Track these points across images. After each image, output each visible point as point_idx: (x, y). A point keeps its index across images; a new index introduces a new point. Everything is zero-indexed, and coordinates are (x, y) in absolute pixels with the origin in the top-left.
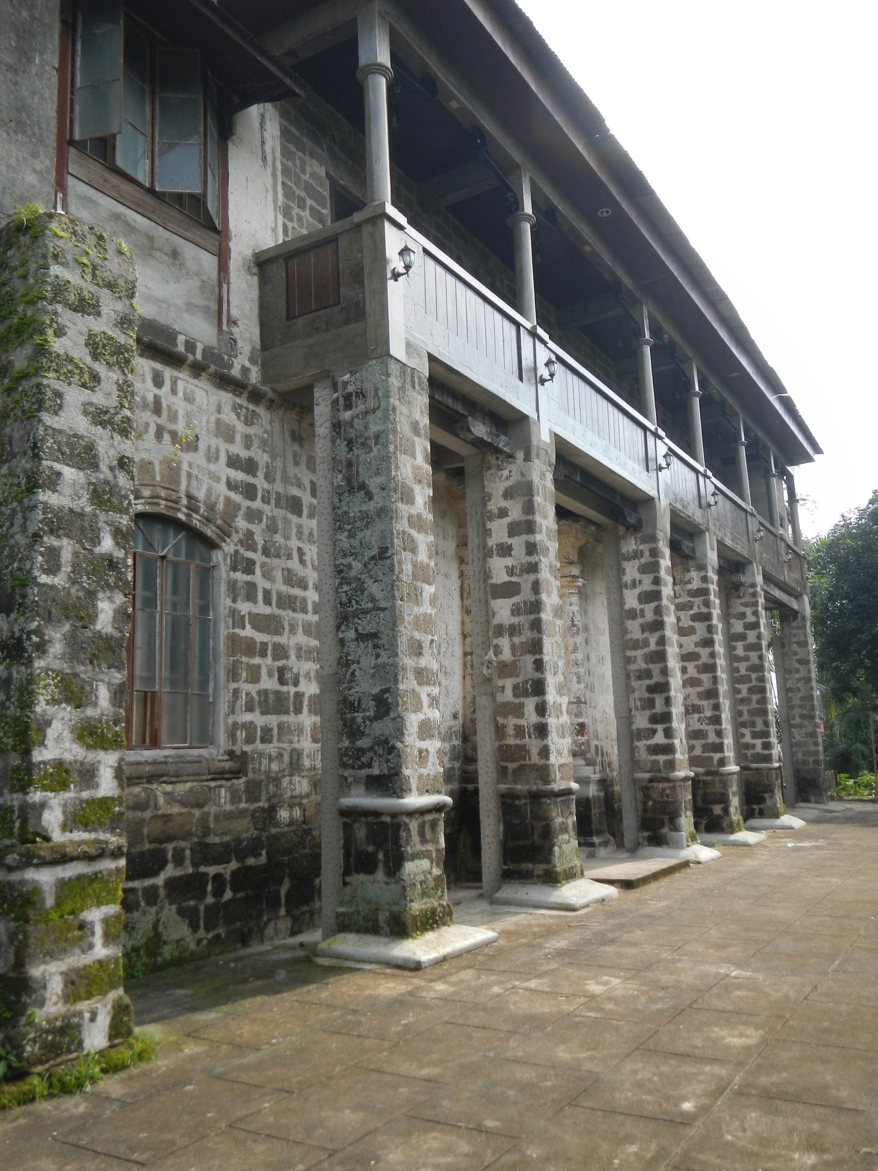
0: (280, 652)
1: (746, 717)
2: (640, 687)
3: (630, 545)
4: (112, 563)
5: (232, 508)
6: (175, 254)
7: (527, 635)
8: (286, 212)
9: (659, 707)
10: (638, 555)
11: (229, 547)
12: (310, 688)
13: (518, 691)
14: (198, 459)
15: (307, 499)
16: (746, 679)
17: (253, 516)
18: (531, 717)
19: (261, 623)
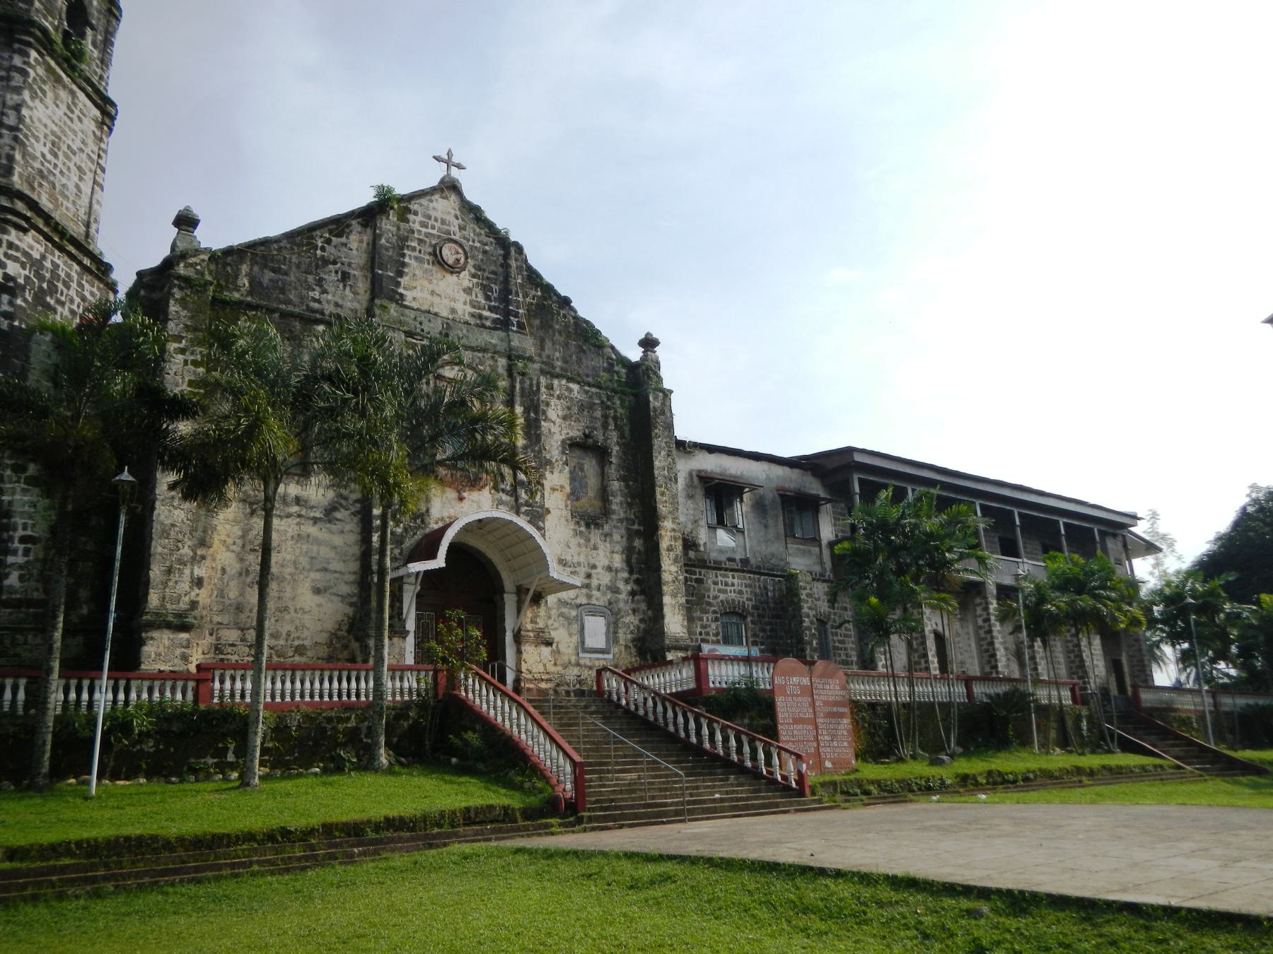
0: (846, 649)
1: (1074, 670)
2: (986, 655)
3: (978, 600)
4: (814, 634)
5: (830, 612)
6: (810, 551)
7: (920, 640)
8: (835, 525)
9: (993, 663)
10: (981, 604)
11: (830, 623)
12: (855, 659)
13: (919, 657)
14: (821, 602)
15: (848, 606)
16: (1073, 651)
17: (835, 614)
18: (923, 665)
19: (840, 642)
